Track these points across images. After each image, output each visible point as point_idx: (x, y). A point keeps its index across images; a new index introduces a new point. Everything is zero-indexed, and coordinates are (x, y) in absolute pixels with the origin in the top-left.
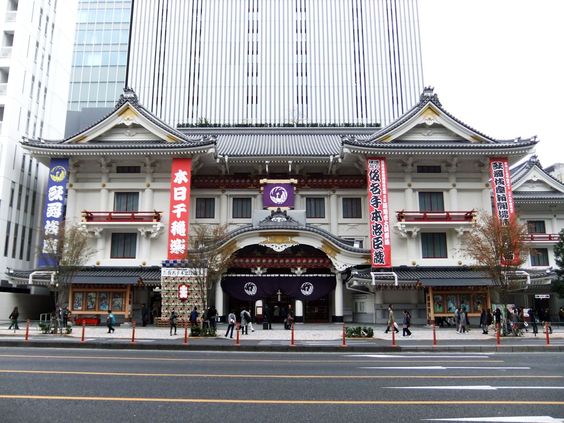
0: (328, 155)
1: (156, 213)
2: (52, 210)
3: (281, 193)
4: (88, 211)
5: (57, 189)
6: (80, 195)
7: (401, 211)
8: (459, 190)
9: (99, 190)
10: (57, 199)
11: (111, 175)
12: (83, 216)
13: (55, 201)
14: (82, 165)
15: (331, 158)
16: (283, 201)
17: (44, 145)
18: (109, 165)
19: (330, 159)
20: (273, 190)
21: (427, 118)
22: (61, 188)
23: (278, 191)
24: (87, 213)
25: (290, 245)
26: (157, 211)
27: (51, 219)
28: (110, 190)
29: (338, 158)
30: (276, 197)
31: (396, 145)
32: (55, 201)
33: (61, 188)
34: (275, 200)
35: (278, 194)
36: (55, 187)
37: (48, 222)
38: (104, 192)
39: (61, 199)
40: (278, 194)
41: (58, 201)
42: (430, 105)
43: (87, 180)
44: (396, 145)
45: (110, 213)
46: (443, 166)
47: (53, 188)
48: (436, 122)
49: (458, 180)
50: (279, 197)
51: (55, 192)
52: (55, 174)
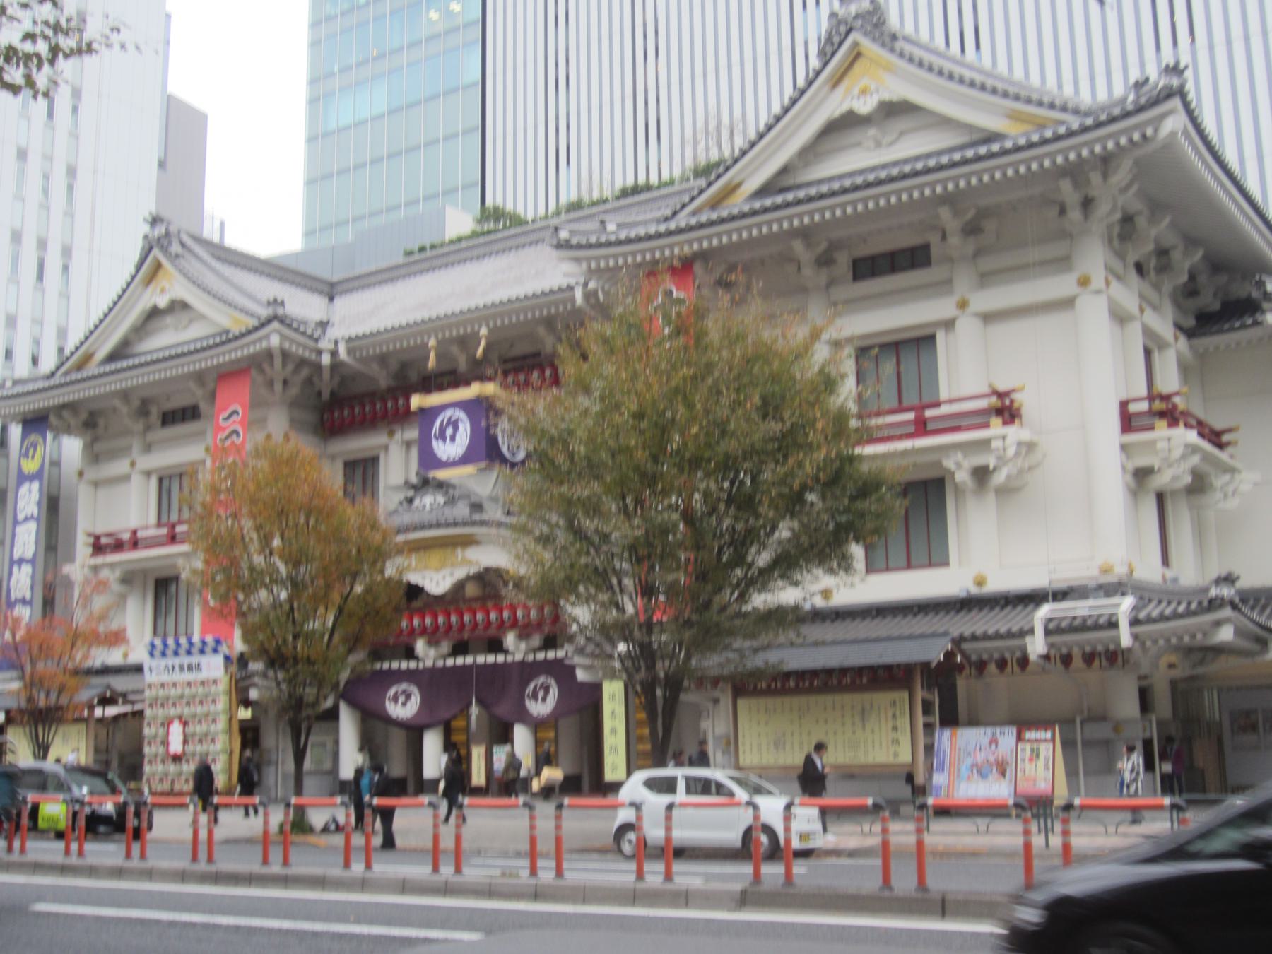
0: (570, 288)
6: (102, 492)
8: (988, 318)
9: (126, 478)
11: (151, 437)
14: (101, 422)
15: (578, 295)
17: (10, 393)
18: (143, 410)
19: (573, 300)
21: (856, 91)
24: (97, 538)
25: (460, 573)
27: (21, 561)
28: (148, 474)
29: (595, 293)
31: (768, 202)
32: (26, 519)
37: (15, 569)
38: (137, 479)
42: (856, 44)
43: (114, 455)
44: (768, 202)
45: (134, 532)
46: (934, 239)
48: (886, 96)
49: (985, 279)
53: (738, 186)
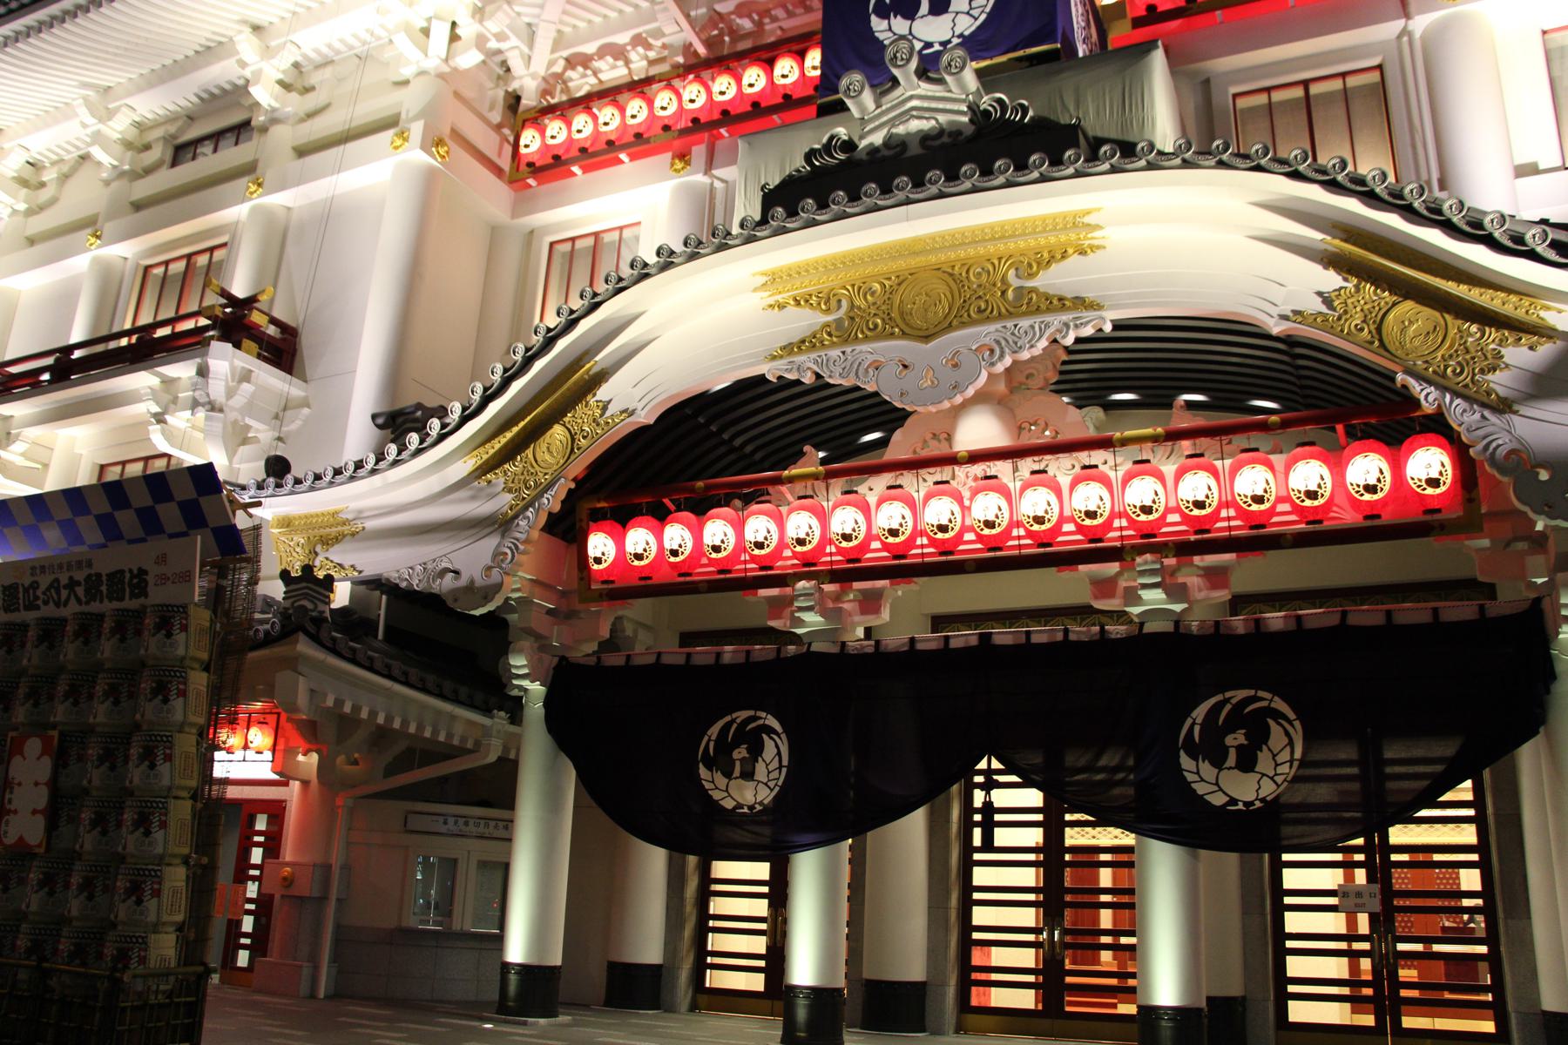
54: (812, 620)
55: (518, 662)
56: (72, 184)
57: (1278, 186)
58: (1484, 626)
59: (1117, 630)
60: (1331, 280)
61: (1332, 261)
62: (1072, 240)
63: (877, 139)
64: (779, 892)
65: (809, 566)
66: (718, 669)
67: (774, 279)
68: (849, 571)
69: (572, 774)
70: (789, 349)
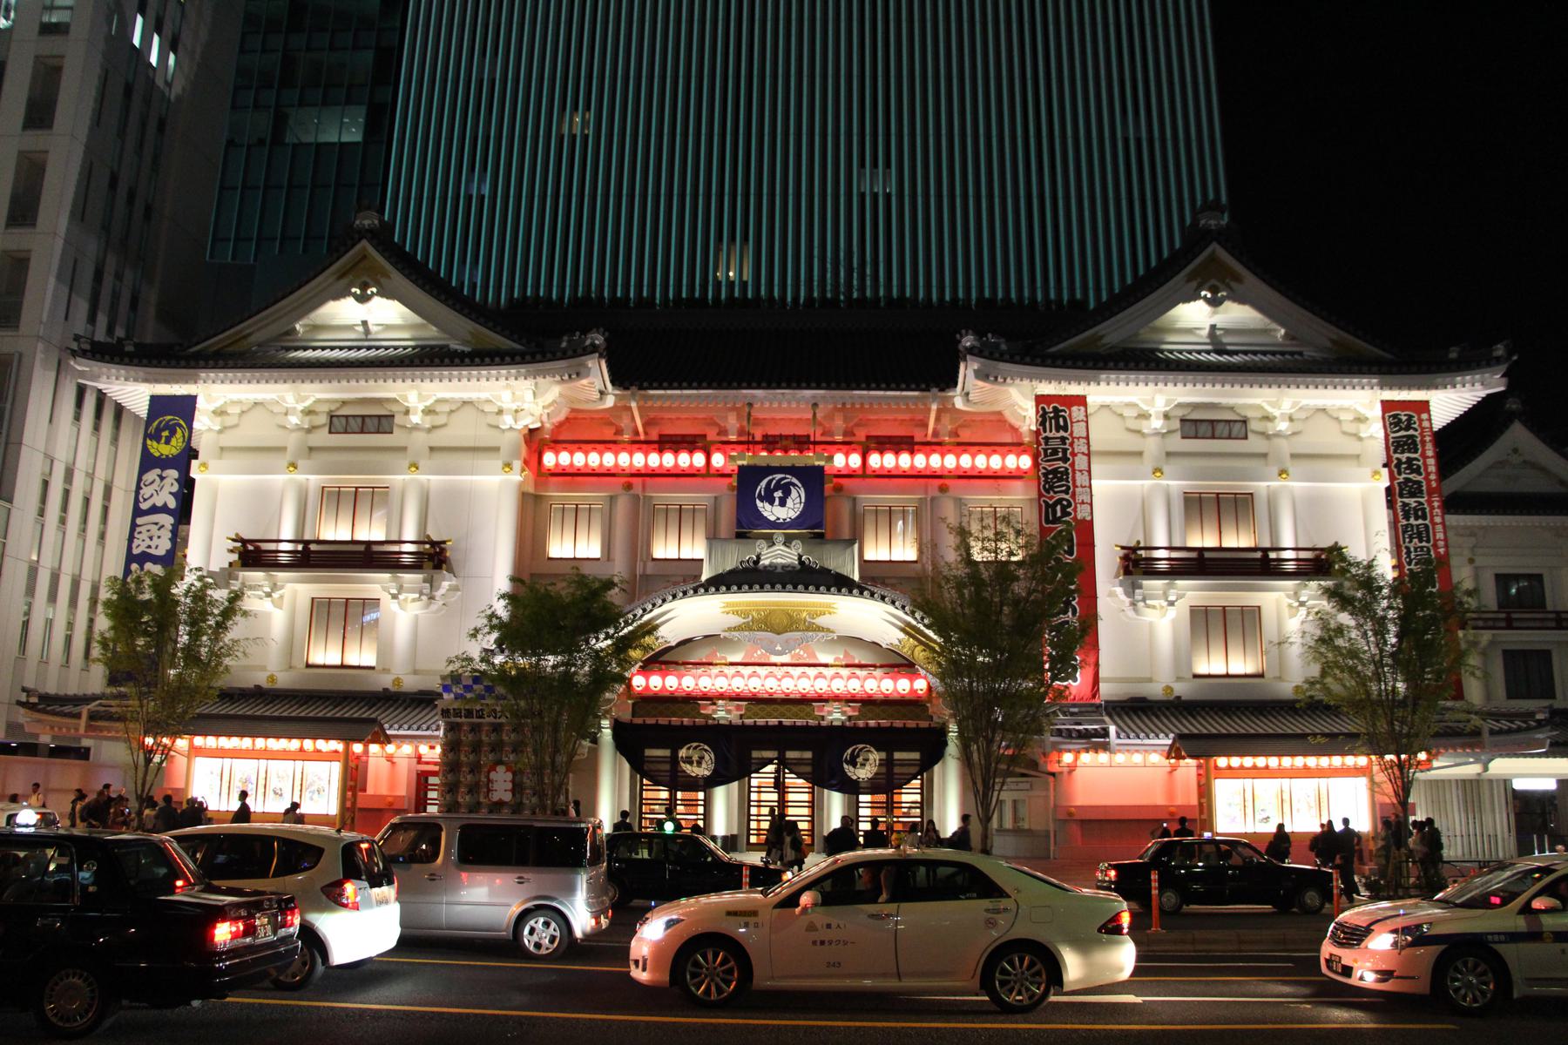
1: (433, 544)
2: (145, 536)
3: (787, 493)
4: (246, 537)
5: (162, 478)
7: (1132, 544)
10: (159, 504)
12: (231, 551)
13: (154, 510)
16: (793, 515)
20: (764, 483)
22: (173, 474)
23: (778, 486)
24: (244, 542)
26: (435, 538)
30: (772, 503)
32: (154, 510)
33: (173, 474)
34: (772, 512)
35: (778, 494)
36: (158, 471)
39: (172, 504)
40: (778, 494)
41: (164, 509)
47: (152, 475)
50: (783, 503)
51: (155, 486)
52: (157, 437)
53: (1101, 337)
54: (721, 714)
55: (605, 723)
56: (245, 417)
57: (891, 608)
58: (930, 729)
59: (824, 723)
60: (902, 635)
61: (903, 630)
62: (828, 610)
63: (767, 562)
64: (708, 803)
65: (722, 696)
66: (682, 727)
67: (728, 605)
68: (736, 698)
69: (627, 766)
70: (730, 629)
